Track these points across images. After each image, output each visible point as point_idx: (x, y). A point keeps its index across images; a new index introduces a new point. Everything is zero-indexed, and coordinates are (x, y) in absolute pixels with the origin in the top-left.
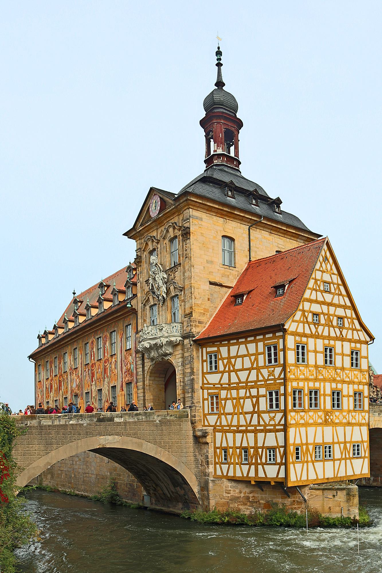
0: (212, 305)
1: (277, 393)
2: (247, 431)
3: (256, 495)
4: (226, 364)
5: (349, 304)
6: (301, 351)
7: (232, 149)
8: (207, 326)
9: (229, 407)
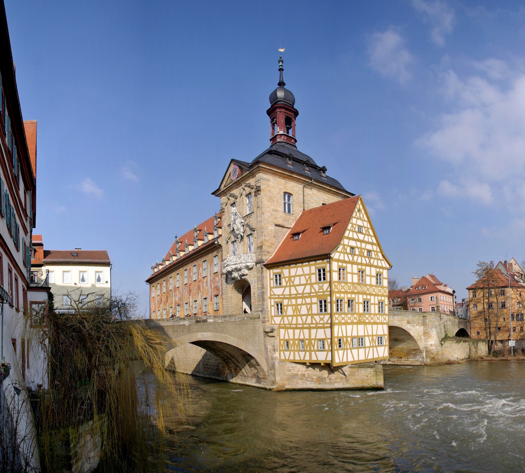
1: (325, 302)
2: (303, 328)
3: (310, 373)
5: (375, 242)
7: (290, 131)
8: (273, 255)
9: (290, 311)
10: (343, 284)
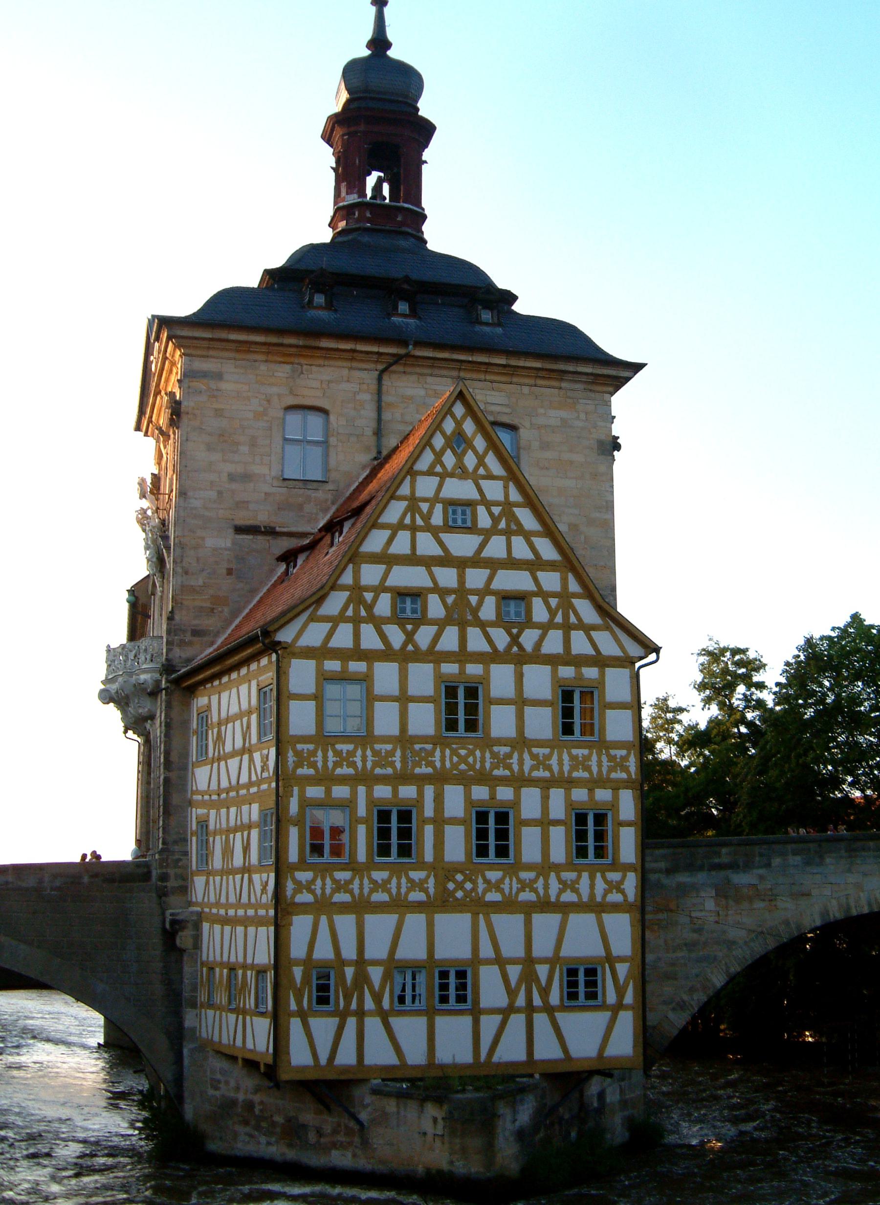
4: (217, 739)
8: (219, 641)
10: (345, 747)
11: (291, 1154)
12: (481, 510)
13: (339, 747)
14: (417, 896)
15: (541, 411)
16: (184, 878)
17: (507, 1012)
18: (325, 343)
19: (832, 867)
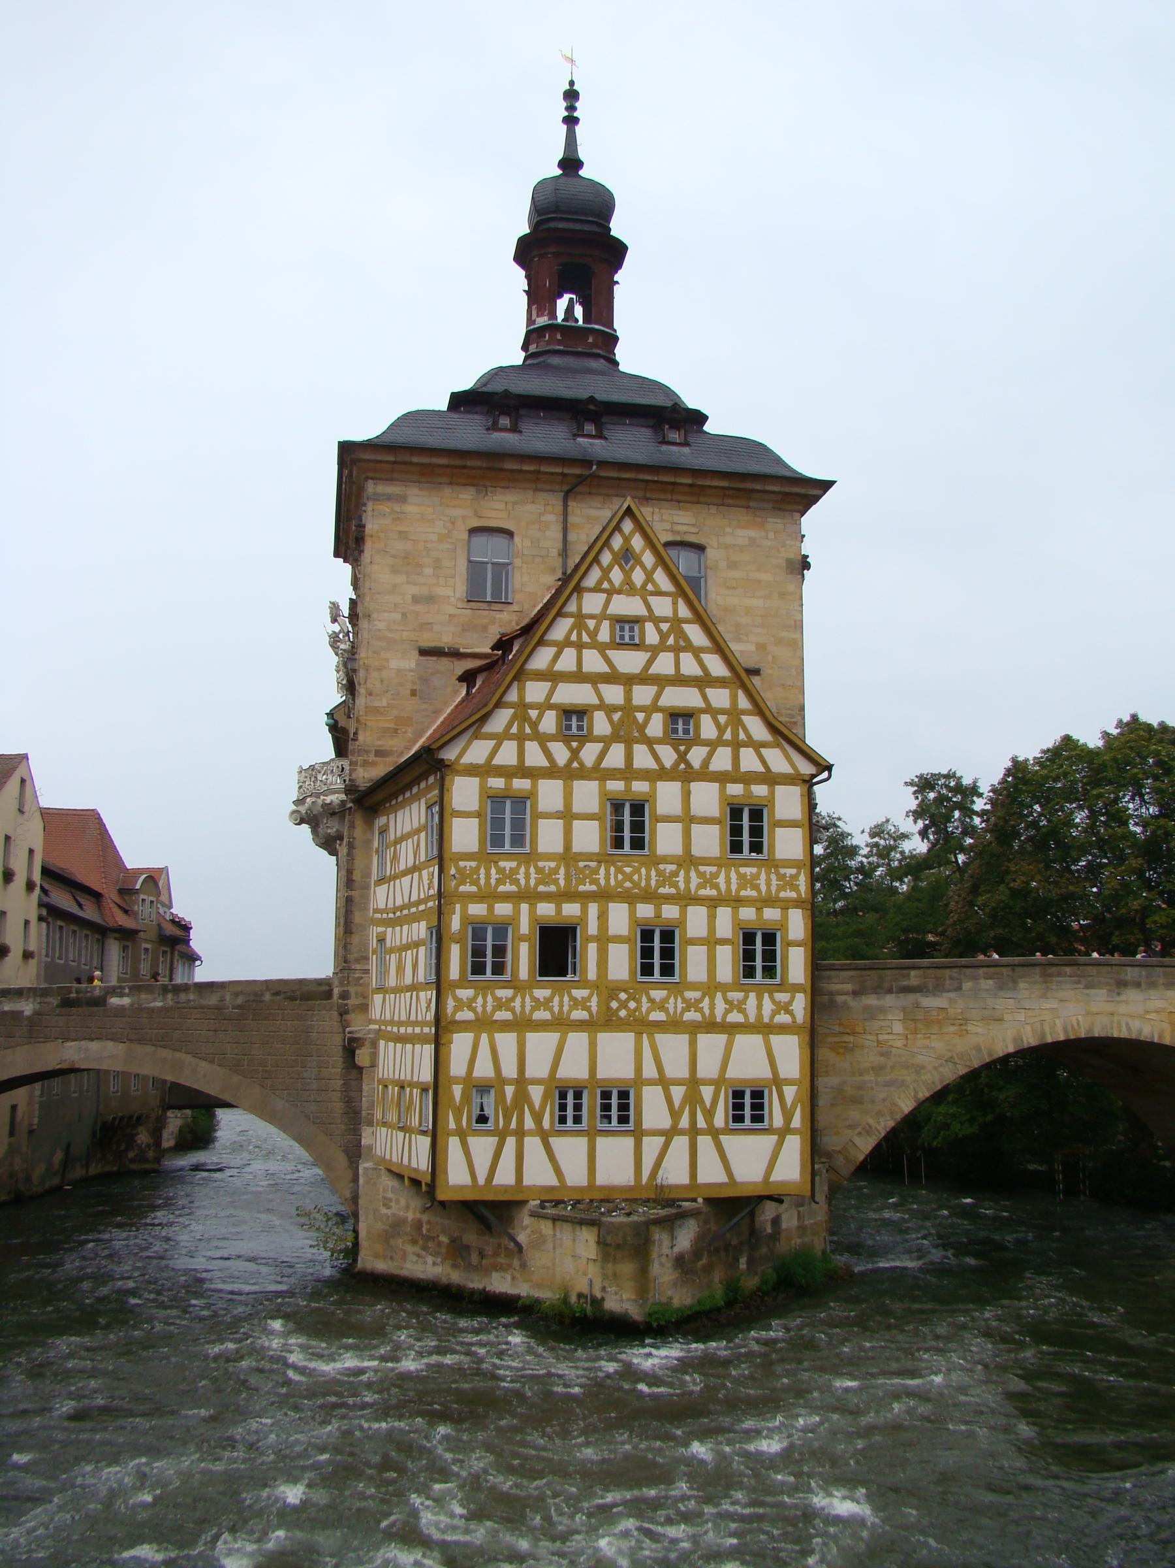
0: (425, 706)
6: (509, 819)
11: (456, 1277)
12: (649, 627)
13: (502, 864)
14: (579, 1014)
15: (728, 530)
16: (365, 996)
17: (669, 1134)
18: (508, 465)
19: (1027, 992)
